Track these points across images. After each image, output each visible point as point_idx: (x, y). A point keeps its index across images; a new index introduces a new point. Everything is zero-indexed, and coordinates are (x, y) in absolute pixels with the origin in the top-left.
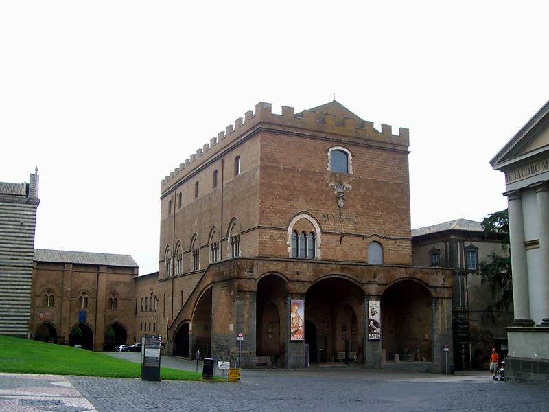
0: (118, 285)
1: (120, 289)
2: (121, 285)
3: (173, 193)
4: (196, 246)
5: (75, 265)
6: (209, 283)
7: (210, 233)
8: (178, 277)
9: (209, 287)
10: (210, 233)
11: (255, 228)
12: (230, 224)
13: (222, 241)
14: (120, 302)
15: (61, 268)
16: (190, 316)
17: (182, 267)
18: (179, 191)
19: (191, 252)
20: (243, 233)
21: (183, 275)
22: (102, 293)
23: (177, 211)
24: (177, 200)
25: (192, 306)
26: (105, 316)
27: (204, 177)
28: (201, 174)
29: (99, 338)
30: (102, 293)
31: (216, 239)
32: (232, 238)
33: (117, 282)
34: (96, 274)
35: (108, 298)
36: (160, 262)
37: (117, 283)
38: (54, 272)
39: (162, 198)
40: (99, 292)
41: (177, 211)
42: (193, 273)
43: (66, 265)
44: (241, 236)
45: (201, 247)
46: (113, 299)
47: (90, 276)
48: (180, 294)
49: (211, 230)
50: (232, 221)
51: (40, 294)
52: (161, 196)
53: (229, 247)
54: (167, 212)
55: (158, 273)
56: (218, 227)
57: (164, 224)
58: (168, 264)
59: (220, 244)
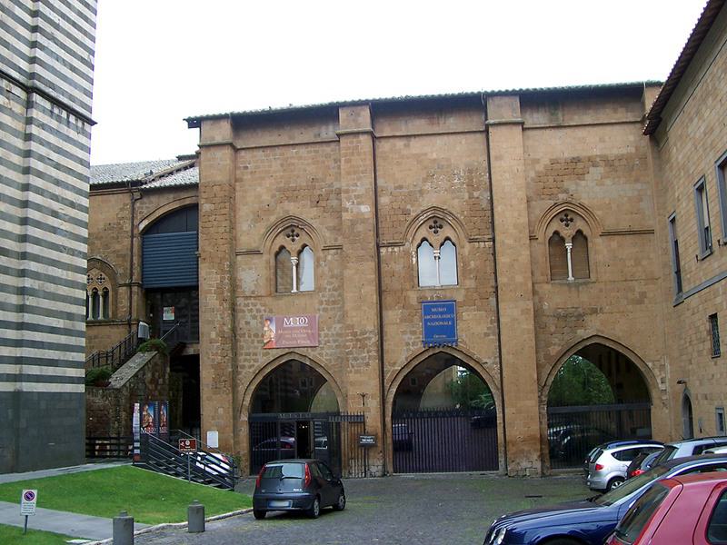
0: (581, 176)
1: (591, 191)
2: (595, 173)
5: (384, 110)
14: (600, 249)
15: (328, 132)
22: (511, 215)
26: (537, 313)
29: (522, 416)
30: (511, 215)
33: (576, 160)
34: (484, 135)
35: (544, 234)
37: (576, 167)
38: (303, 151)
40: (498, 209)
43: (342, 114)
46: (566, 240)
47: (450, 149)
51: (254, 246)
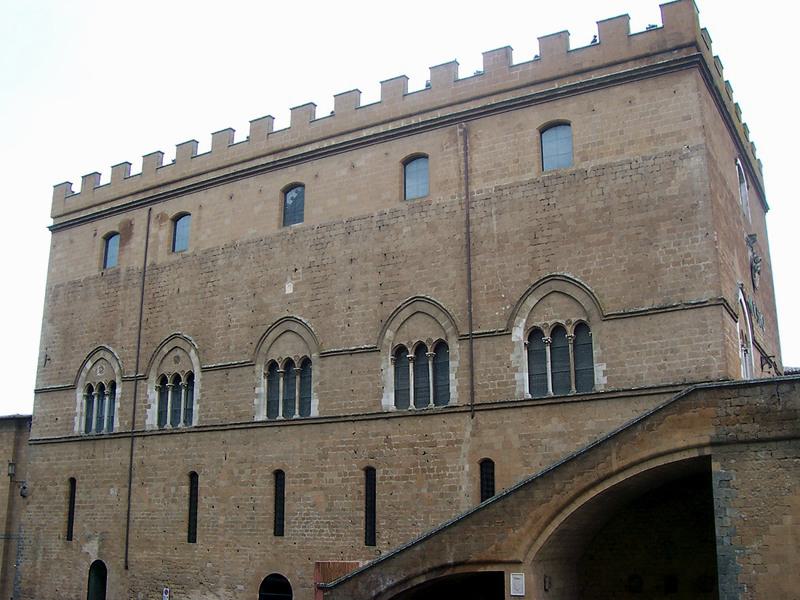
3: (139, 217)
4: (287, 348)
6: (681, 444)
7: (392, 317)
8: (161, 432)
9: (695, 454)
10: (392, 317)
11: (700, 305)
12: (527, 293)
13: (470, 338)
16: (523, 548)
17: (196, 407)
18: (171, 208)
19: (261, 369)
20: (607, 318)
21: (200, 429)
23: (162, 256)
24: (162, 233)
25: (543, 511)
27: (344, 172)
28: (333, 169)
31: (422, 331)
32: (534, 334)
36: (37, 392)
39: (54, 229)
41: (162, 256)
42: (262, 425)
44: (599, 332)
45: (323, 356)
48: (186, 479)
49: (399, 310)
50: (536, 286)
52: (51, 222)
53: (520, 357)
54: (95, 261)
55: (29, 419)
56: (451, 300)
57: (62, 299)
58: (99, 393)
59: (455, 347)
